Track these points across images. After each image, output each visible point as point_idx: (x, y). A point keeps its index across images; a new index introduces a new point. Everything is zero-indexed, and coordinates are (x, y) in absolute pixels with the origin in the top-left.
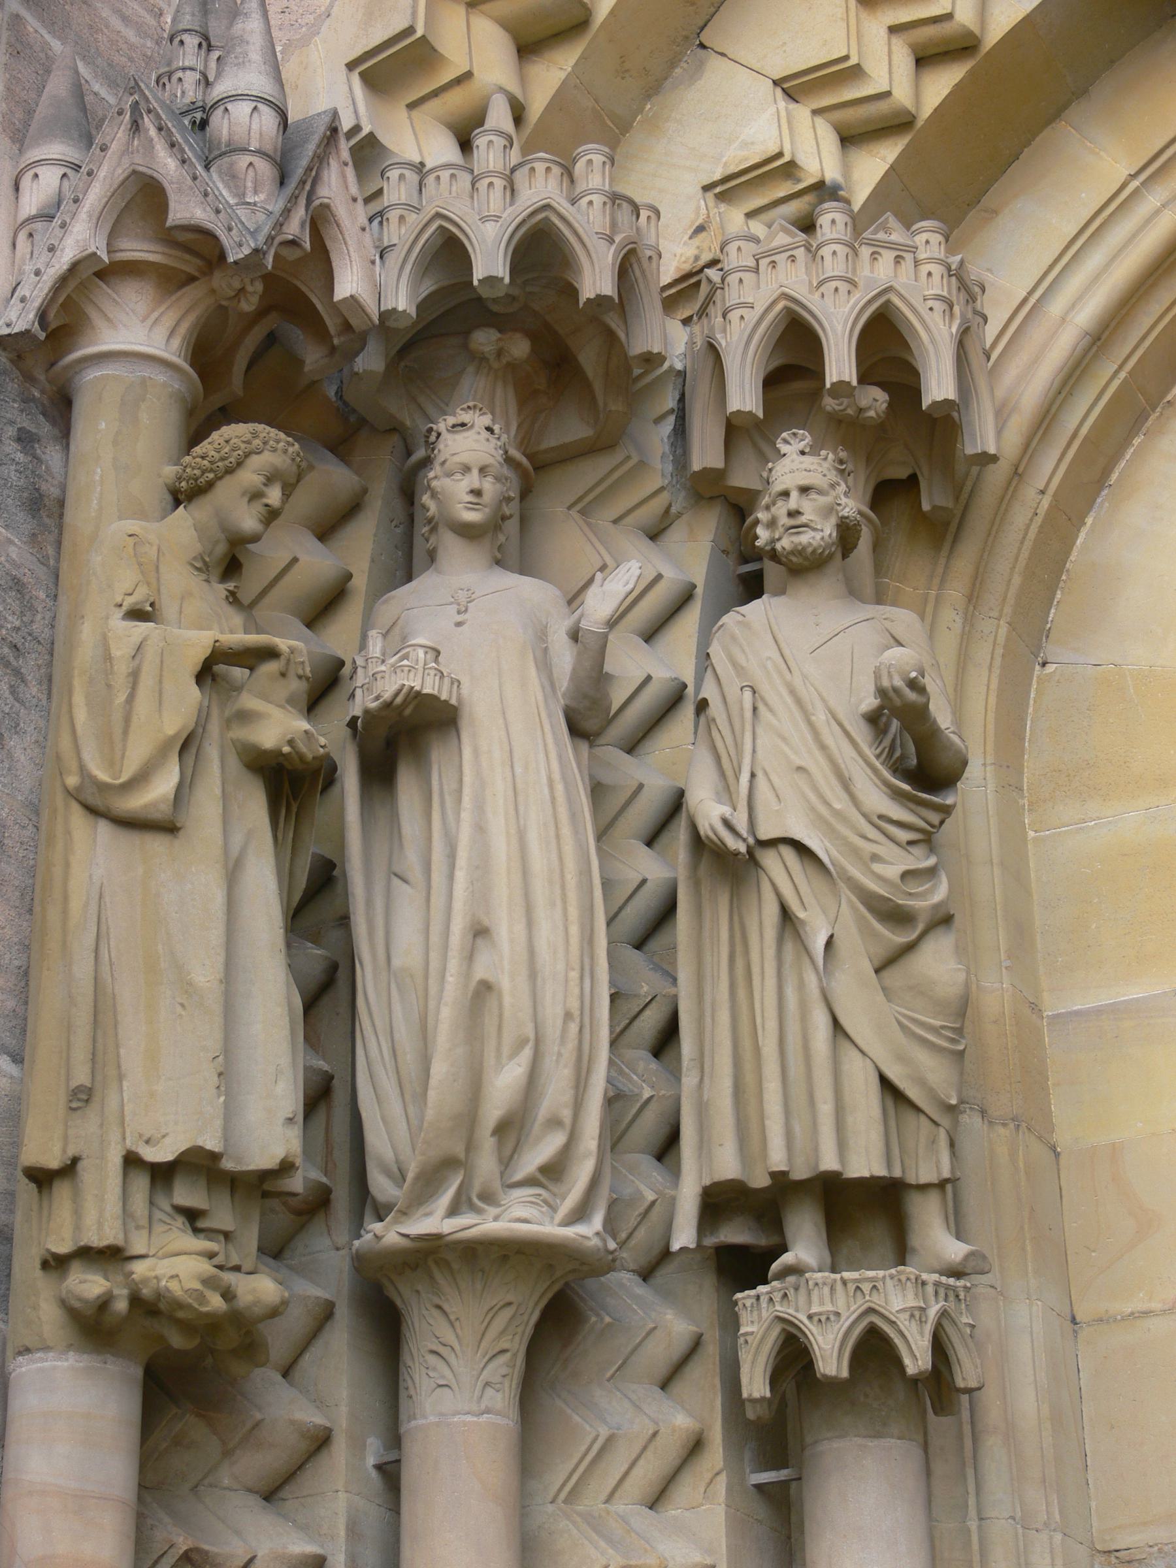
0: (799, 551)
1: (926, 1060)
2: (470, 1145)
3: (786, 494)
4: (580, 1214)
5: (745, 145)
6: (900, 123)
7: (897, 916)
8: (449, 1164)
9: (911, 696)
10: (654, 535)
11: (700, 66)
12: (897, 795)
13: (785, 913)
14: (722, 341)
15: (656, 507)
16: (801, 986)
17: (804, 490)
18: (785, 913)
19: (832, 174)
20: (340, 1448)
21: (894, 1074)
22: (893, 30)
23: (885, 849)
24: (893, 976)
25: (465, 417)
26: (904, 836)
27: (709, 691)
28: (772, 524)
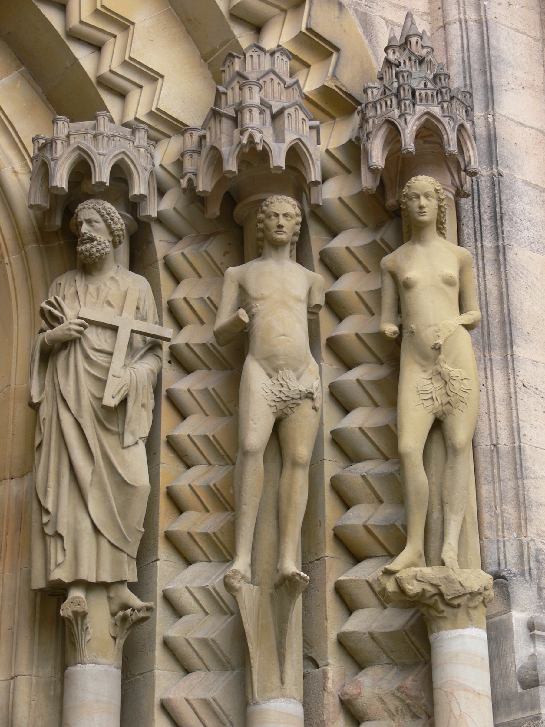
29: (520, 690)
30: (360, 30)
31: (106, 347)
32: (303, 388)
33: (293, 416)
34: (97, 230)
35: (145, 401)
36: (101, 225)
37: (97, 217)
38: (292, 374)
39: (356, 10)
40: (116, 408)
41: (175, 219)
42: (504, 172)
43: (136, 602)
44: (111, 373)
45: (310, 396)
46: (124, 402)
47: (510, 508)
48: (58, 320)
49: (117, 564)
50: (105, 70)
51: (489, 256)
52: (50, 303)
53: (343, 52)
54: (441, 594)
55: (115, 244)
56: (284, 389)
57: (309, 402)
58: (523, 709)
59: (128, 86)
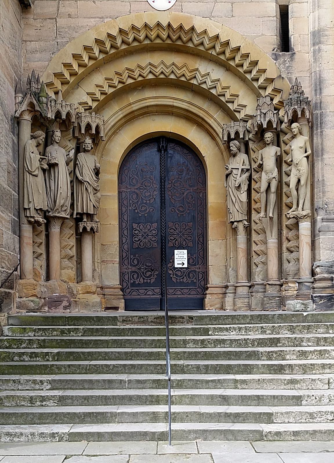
0: (88, 150)
1: (96, 203)
2: (59, 208)
3: (87, 143)
4: (68, 215)
5: (83, 99)
6: (99, 101)
7: (96, 190)
8: (58, 209)
9: (99, 169)
10: (69, 141)
11: (78, 88)
12: (96, 178)
13: (86, 188)
14: (81, 124)
15: (70, 138)
16: (87, 195)
17: (89, 143)
18: (86, 188)
19: (91, 105)
20: (43, 232)
21: (94, 204)
22: (99, 90)
23: (95, 183)
24: (95, 195)
25: (58, 130)
26: (96, 182)
27: (78, 162)
28: (85, 146)
29: (318, 233)
30: (289, 83)
31: (237, 174)
32: (273, 176)
33: (271, 183)
34: (233, 148)
35: (245, 183)
36: (234, 146)
37: (233, 145)
38: (271, 174)
39: (287, 78)
40: (238, 187)
41: (252, 138)
42: (324, 111)
43: (246, 223)
44: (237, 179)
45: (274, 178)
46: (240, 185)
47: (321, 194)
48: (228, 169)
49: (242, 216)
50: (234, 108)
51: (319, 134)
52: (226, 166)
53: (283, 91)
54: (298, 217)
55: (239, 150)
56: (269, 177)
57: (274, 179)
58: (318, 237)
59: (240, 110)
